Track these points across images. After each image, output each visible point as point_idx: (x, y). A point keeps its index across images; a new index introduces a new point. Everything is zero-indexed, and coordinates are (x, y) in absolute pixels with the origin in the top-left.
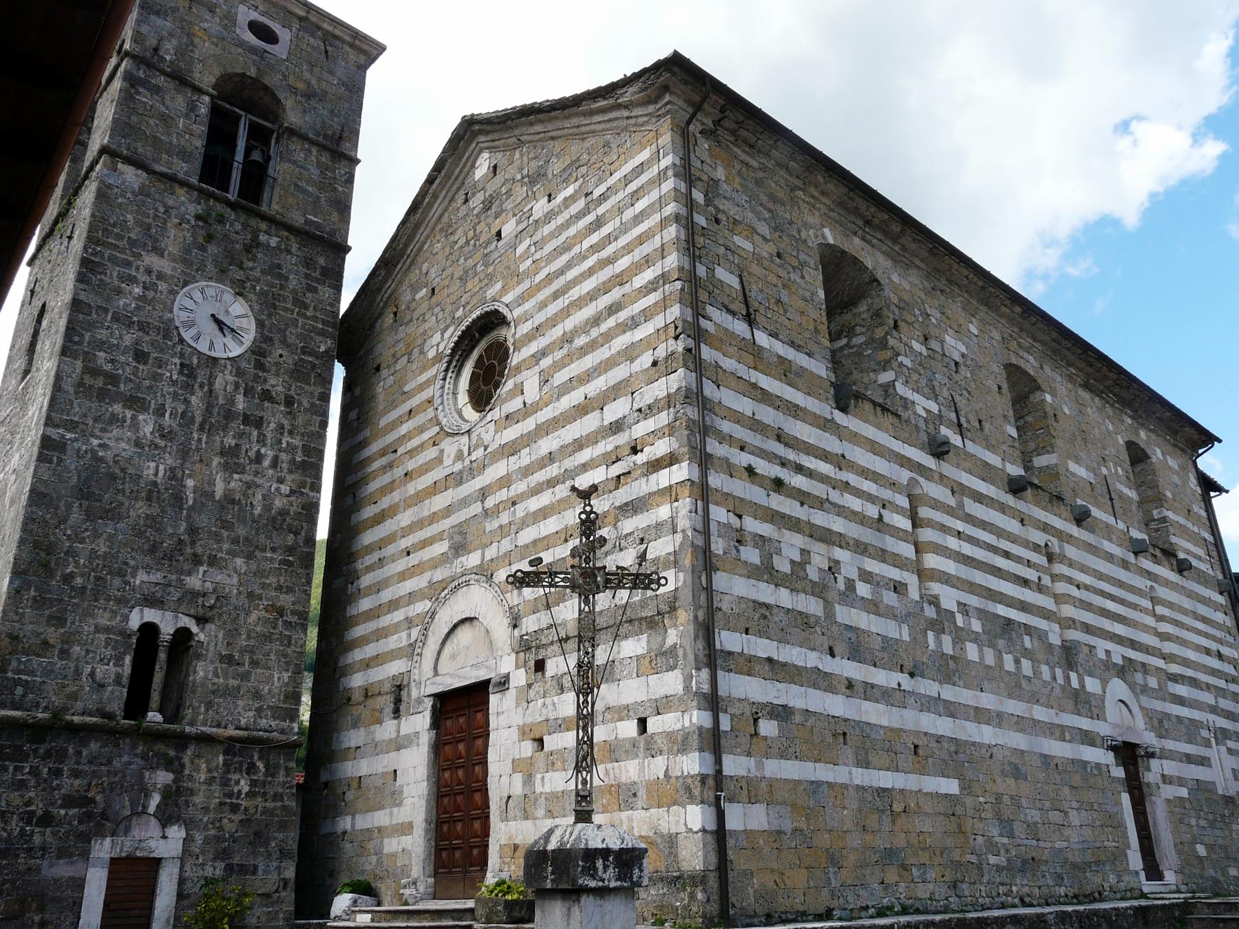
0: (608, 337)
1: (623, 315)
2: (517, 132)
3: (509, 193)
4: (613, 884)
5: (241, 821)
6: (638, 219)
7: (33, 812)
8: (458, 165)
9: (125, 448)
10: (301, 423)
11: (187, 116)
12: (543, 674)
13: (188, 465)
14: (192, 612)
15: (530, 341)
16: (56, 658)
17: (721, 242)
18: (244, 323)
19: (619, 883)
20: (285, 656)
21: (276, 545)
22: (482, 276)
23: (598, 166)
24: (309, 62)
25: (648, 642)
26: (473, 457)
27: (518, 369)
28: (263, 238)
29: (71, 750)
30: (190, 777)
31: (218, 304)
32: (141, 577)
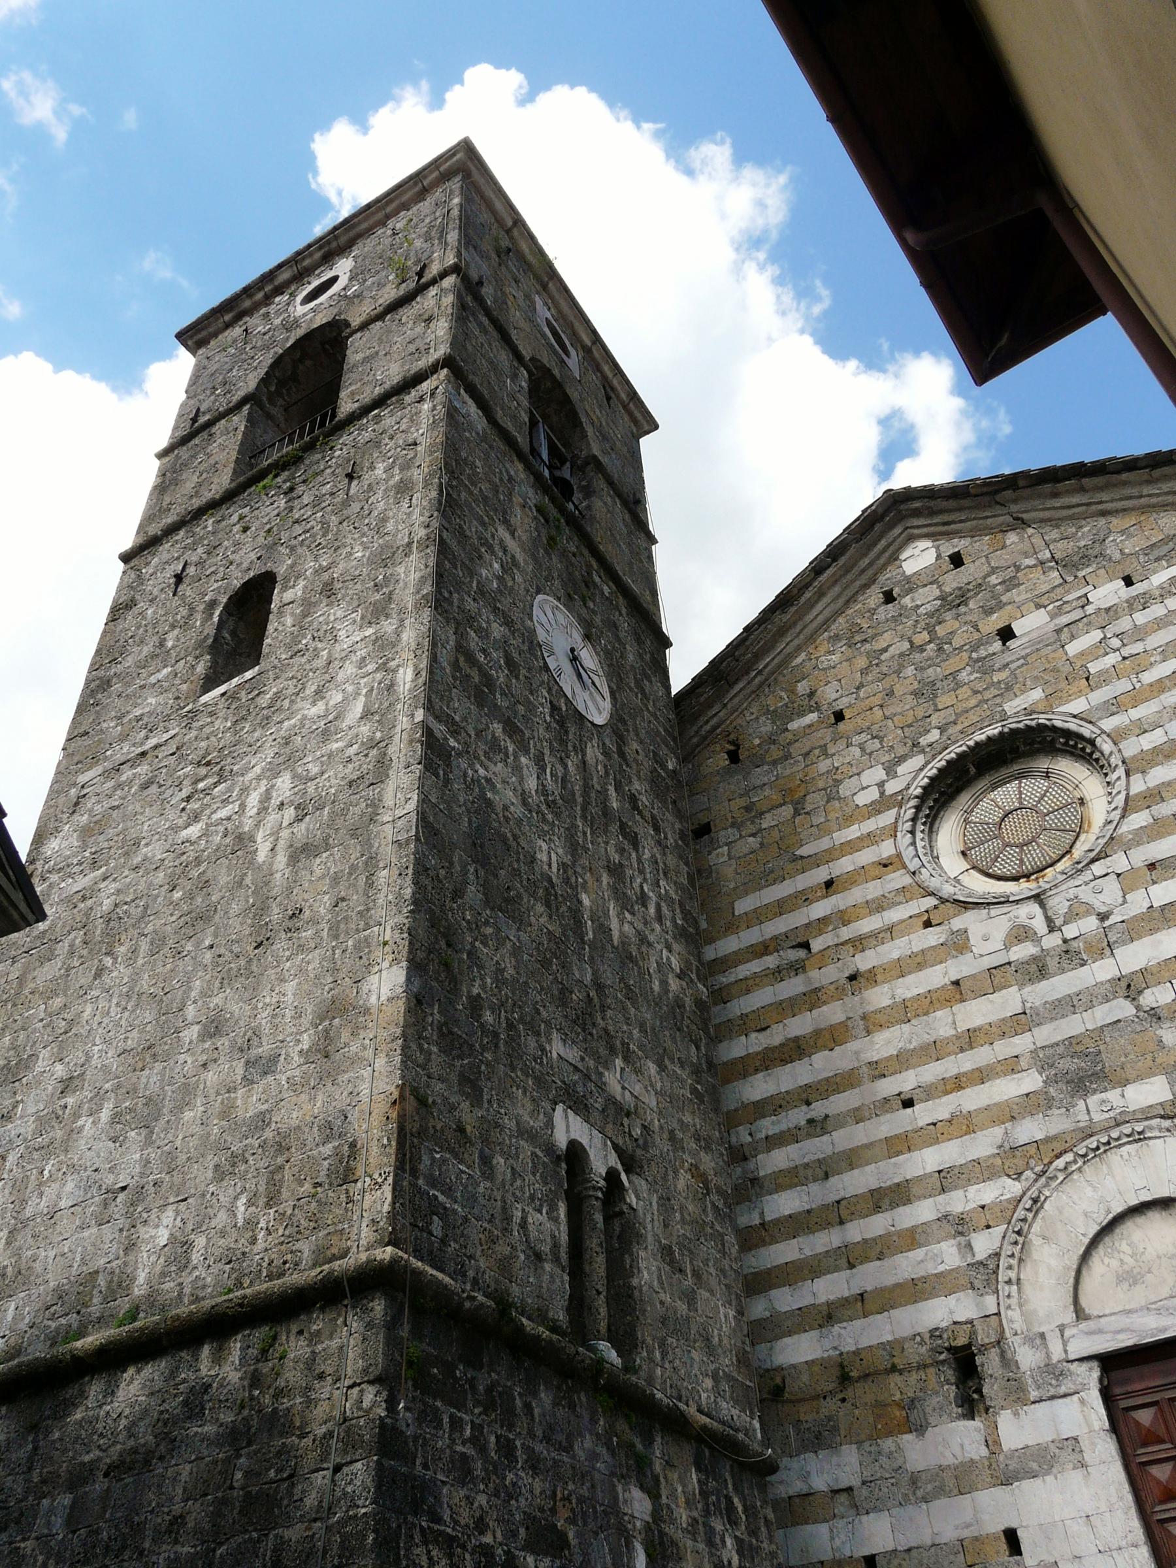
2: (1014, 508)
8: (865, 555)
14: (620, 1142)
26: (1070, 931)
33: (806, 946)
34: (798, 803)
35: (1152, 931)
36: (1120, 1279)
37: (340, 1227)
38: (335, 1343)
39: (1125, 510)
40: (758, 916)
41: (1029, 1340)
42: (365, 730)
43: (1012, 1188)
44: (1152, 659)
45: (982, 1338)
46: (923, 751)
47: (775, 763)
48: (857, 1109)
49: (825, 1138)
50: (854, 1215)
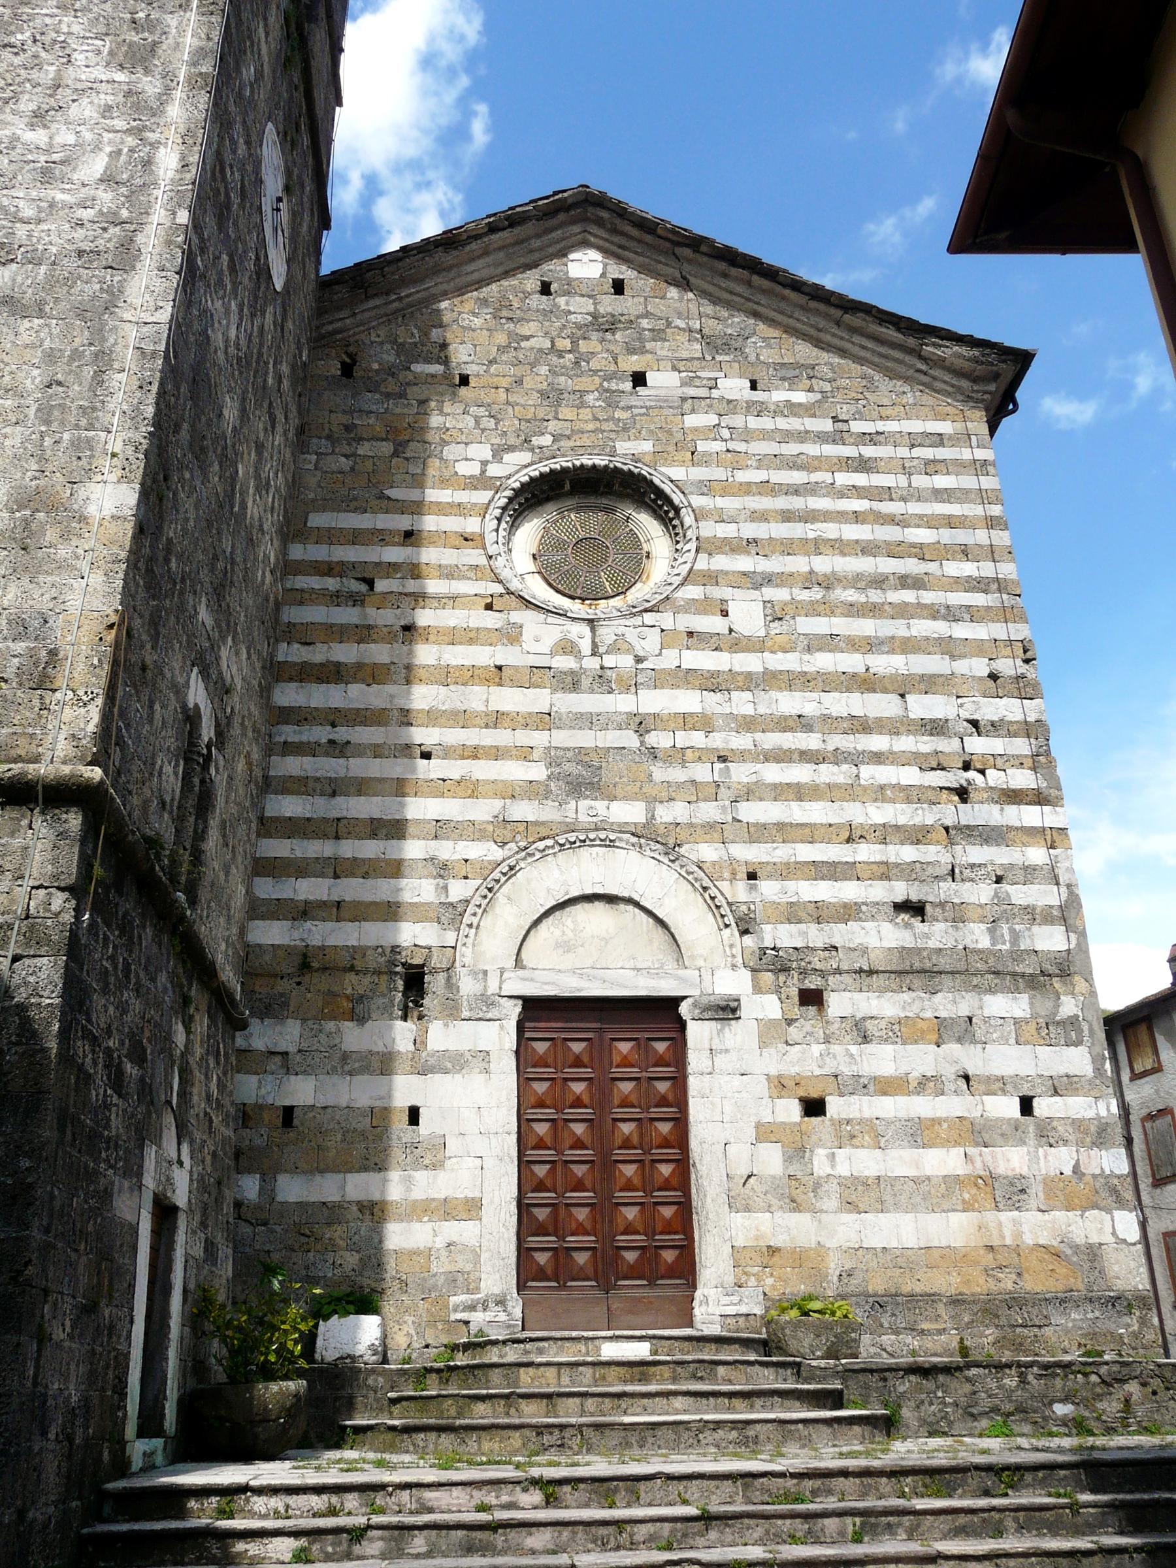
2: (687, 268)
26: (609, 661)
33: (370, 583)
34: (400, 444)
35: (674, 686)
36: (558, 945)
37: (30, 730)
38: (17, 842)
39: (773, 321)
40: (330, 536)
41: (474, 973)
42: (106, 197)
43: (495, 853)
44: (749, 463)
45: (435, 962)
46: (532, 450)
47: (388, 396)
48: (378, 745)
49: (342, 761)
50: (349, 835)
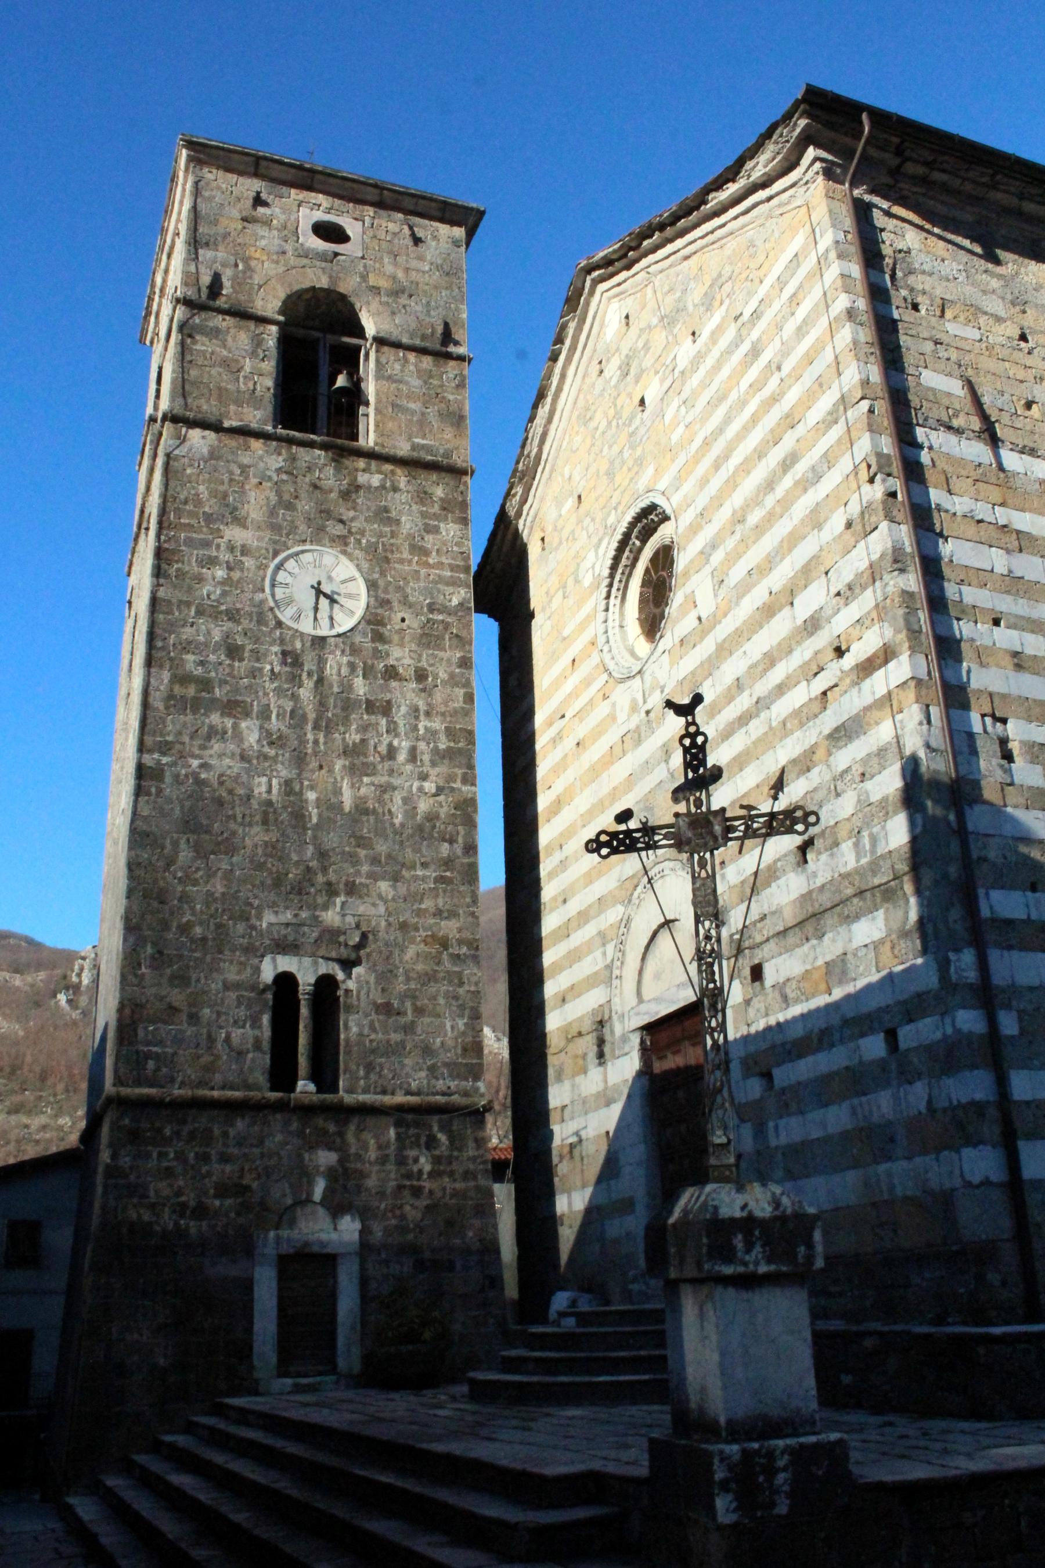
0: (786, 503)
1: (801, 468)
3: (646, 347)
4: (763, 1269)
5: (427, 1207)
6: (801, 331)
7: (184, 1206)
9: (231, 766)
10: (440, 700)
11: (253, 354)
12: (762, 984)
13: (305, 775)
14: (334, 955)
15: (695, 533)
16: (186, 1025)
17: (926, 335)
18: (351, 588)
19: (773, 1267)
20: (456, 998)
21: (428, 859)
22: (630, 463)
23: (744, 276)
24: (390, 252)
25: (886, 919)
27: (686, 574)
28: (362, 478)
29: (217, 1132)
30: (359, 1157)
31: (317, 571)
32: (269, 918)
